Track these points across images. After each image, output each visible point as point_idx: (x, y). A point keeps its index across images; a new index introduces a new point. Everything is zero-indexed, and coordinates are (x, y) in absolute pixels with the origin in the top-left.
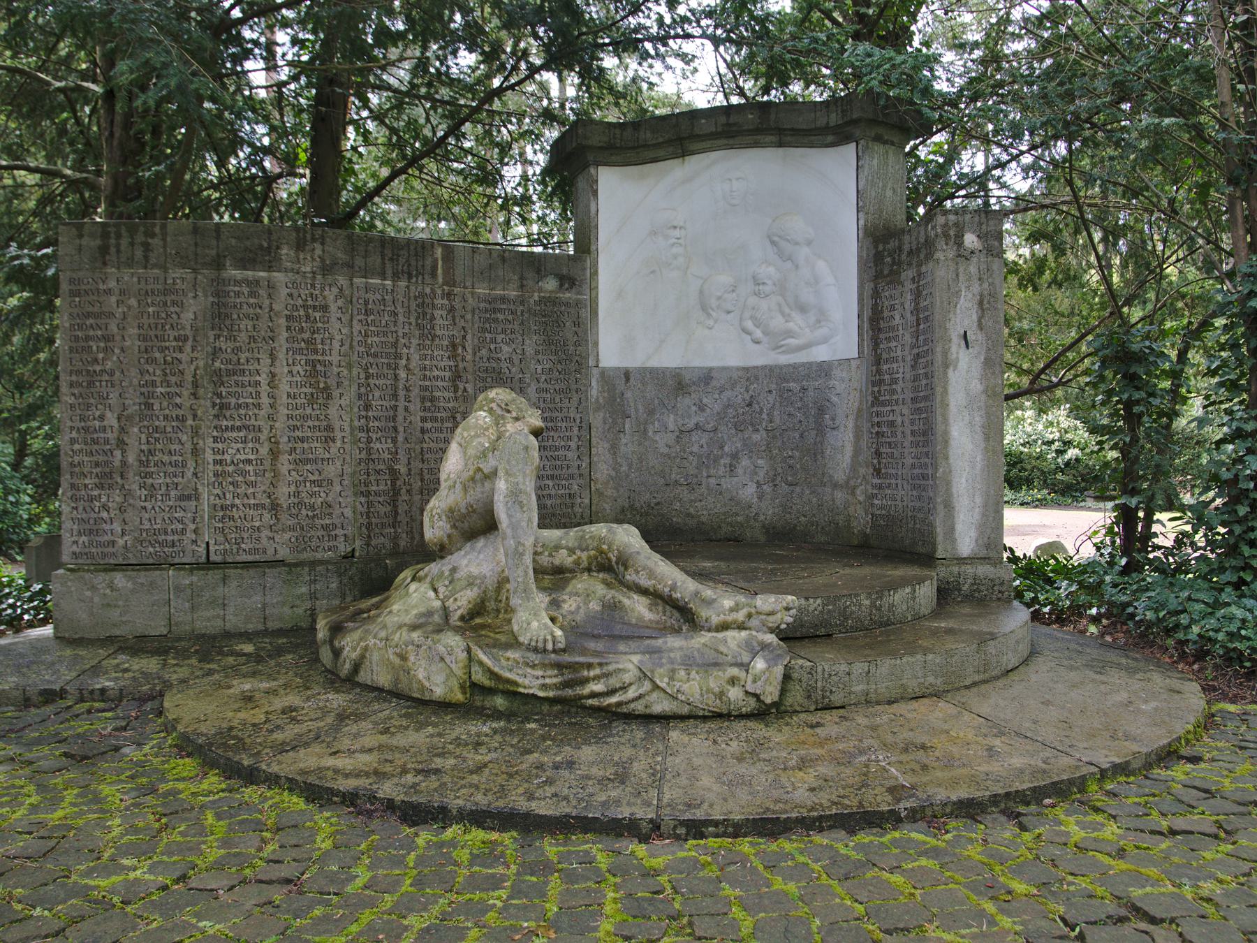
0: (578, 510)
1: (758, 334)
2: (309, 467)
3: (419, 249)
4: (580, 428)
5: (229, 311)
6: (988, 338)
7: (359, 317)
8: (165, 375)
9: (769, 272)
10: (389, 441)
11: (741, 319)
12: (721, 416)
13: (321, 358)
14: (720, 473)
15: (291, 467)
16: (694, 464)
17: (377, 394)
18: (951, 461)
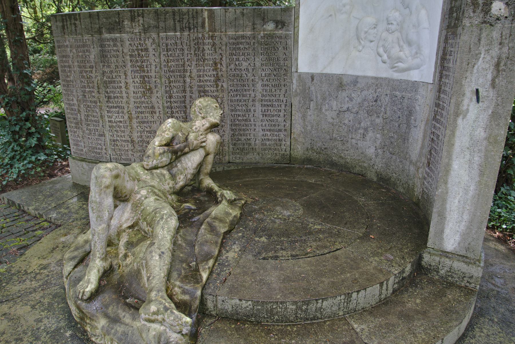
0: (283, 147)
1: (385, 57)
2: (145, 125)
3: (194, 14)
4: (286, 105)
5: (106, 54)
6: (499, 95)
7: (164, 53)
8: (88, 83)
9: (395, 15)
10: (182, 112)
11: (378, 47)
12: (360, 105)
13: (147, 74)
14: (358, 138)
15: (138, 125)
16: (345, 130)
17: (175, 90)
18: (449, 185)
